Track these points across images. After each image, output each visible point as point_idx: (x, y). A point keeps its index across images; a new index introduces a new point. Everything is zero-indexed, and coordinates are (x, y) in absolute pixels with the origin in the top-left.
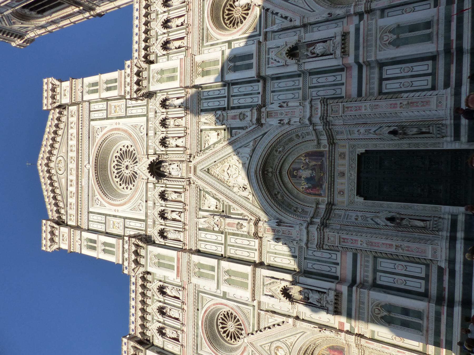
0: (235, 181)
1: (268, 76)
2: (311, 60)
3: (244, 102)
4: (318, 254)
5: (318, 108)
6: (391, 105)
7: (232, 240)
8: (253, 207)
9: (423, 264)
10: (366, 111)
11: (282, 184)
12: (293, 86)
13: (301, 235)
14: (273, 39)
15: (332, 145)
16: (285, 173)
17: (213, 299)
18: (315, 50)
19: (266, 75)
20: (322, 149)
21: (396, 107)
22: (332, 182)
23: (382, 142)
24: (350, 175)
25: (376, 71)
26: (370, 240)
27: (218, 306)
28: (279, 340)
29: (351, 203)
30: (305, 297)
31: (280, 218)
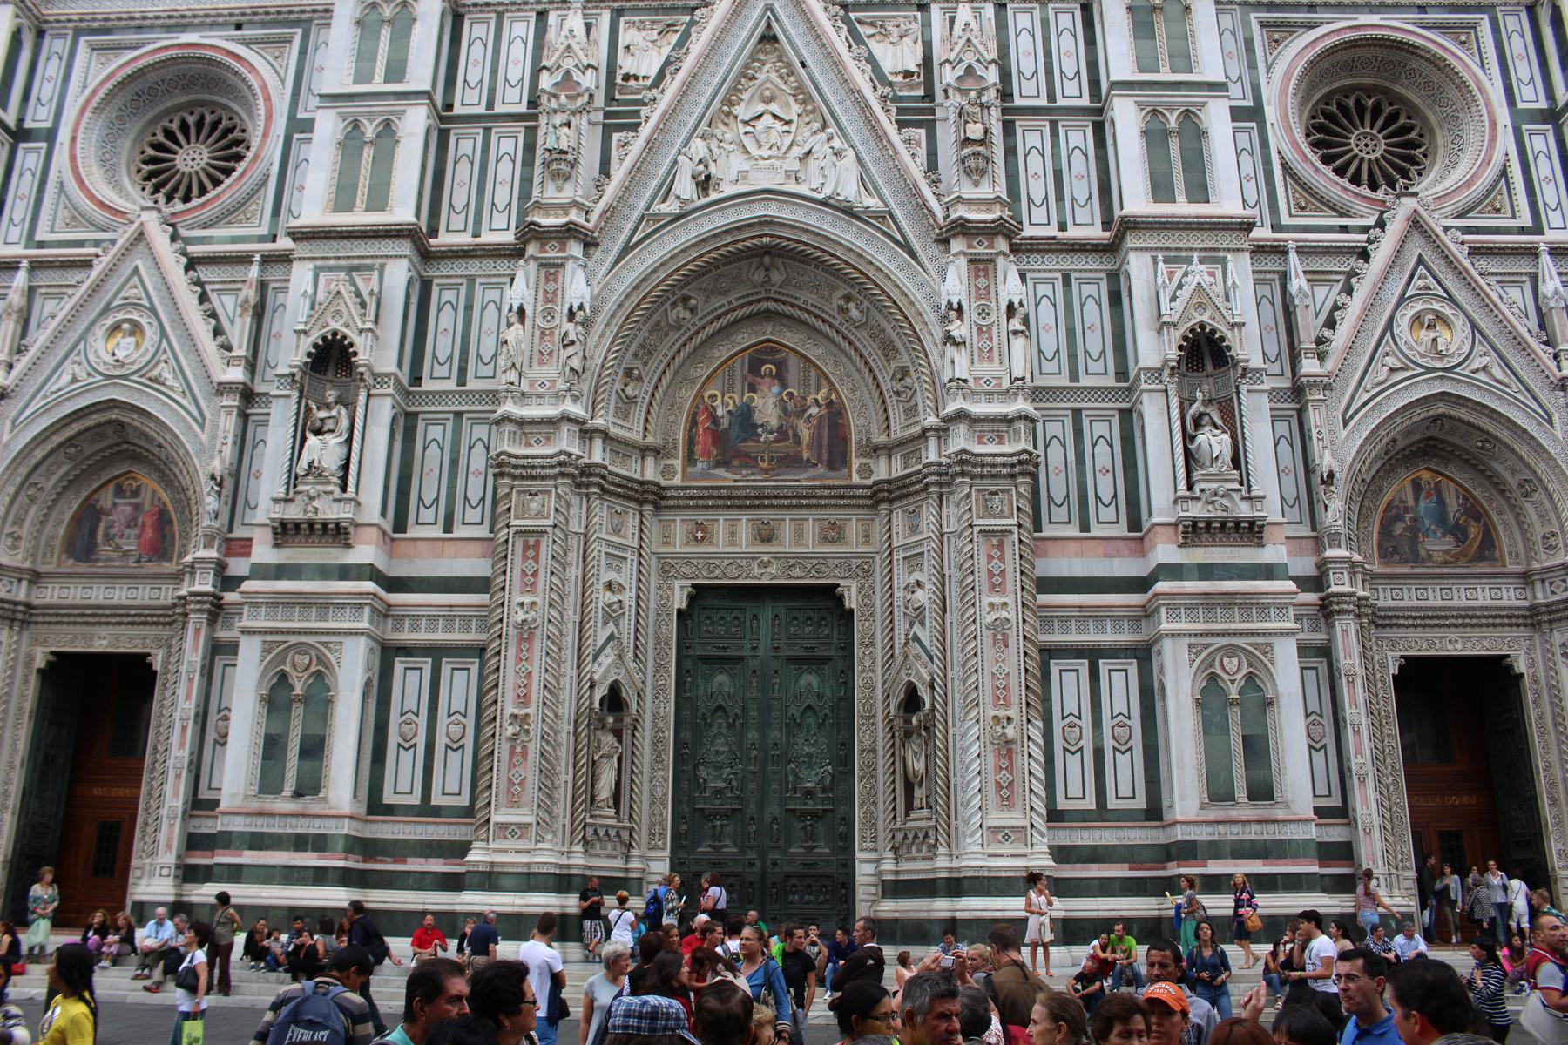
0: (732, 147)
1: (1124, 261)
2: (1175, 414)
3: (1030, 173)
4: (478, 460)
5: (1000, 443)
6: (1004, 688)
7: (508, 144)
8: (636, 215)
9: (473, 799)
10: (988, 609)
11: (723, 321)
12: (1086, 352)
13: (539, 396)
14: (1257, 276)
15: (871, 497)
16: (768, 332)
17: (283, 81)
18: (1208, 428)
19: (1127, 254)
20: (856, 463)
21: (995, 705)
22: (737, 502)
23: (879, 663)
24: (766, 559)
25: (1125, 637)
26: (538, 632)
27: (261, 101)
28: (163, 334)
29: (667, 568)
30: (322, 420)
31: (599, 320)
